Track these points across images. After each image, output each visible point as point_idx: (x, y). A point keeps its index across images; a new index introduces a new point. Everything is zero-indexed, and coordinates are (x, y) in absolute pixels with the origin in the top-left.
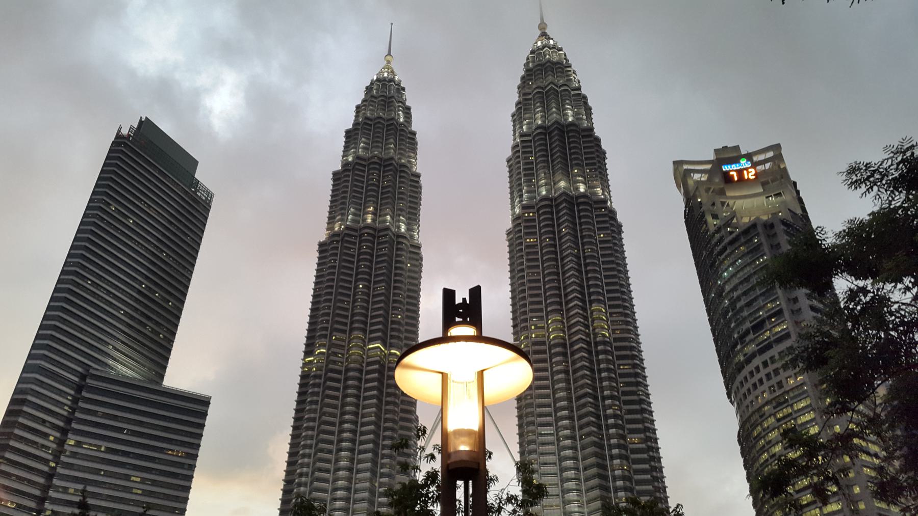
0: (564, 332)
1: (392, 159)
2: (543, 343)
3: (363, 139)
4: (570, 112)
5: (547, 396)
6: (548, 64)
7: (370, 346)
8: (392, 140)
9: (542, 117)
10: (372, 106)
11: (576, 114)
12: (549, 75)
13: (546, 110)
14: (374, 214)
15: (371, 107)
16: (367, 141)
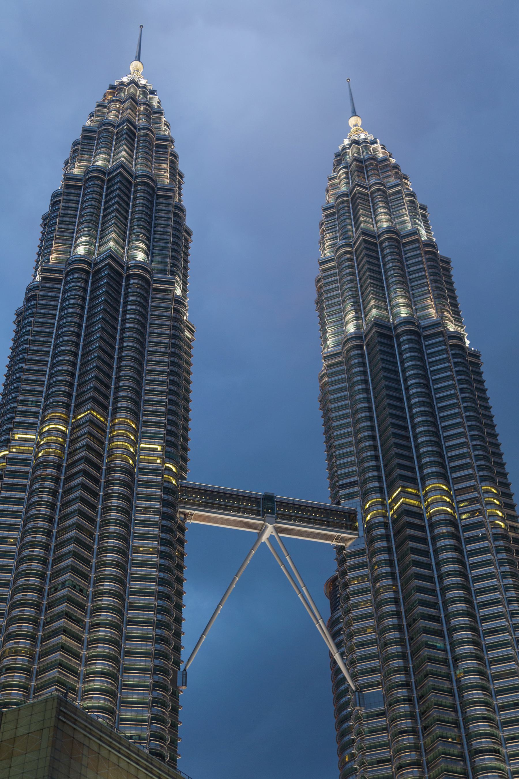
10: (133, 111)
16: (129, 151)
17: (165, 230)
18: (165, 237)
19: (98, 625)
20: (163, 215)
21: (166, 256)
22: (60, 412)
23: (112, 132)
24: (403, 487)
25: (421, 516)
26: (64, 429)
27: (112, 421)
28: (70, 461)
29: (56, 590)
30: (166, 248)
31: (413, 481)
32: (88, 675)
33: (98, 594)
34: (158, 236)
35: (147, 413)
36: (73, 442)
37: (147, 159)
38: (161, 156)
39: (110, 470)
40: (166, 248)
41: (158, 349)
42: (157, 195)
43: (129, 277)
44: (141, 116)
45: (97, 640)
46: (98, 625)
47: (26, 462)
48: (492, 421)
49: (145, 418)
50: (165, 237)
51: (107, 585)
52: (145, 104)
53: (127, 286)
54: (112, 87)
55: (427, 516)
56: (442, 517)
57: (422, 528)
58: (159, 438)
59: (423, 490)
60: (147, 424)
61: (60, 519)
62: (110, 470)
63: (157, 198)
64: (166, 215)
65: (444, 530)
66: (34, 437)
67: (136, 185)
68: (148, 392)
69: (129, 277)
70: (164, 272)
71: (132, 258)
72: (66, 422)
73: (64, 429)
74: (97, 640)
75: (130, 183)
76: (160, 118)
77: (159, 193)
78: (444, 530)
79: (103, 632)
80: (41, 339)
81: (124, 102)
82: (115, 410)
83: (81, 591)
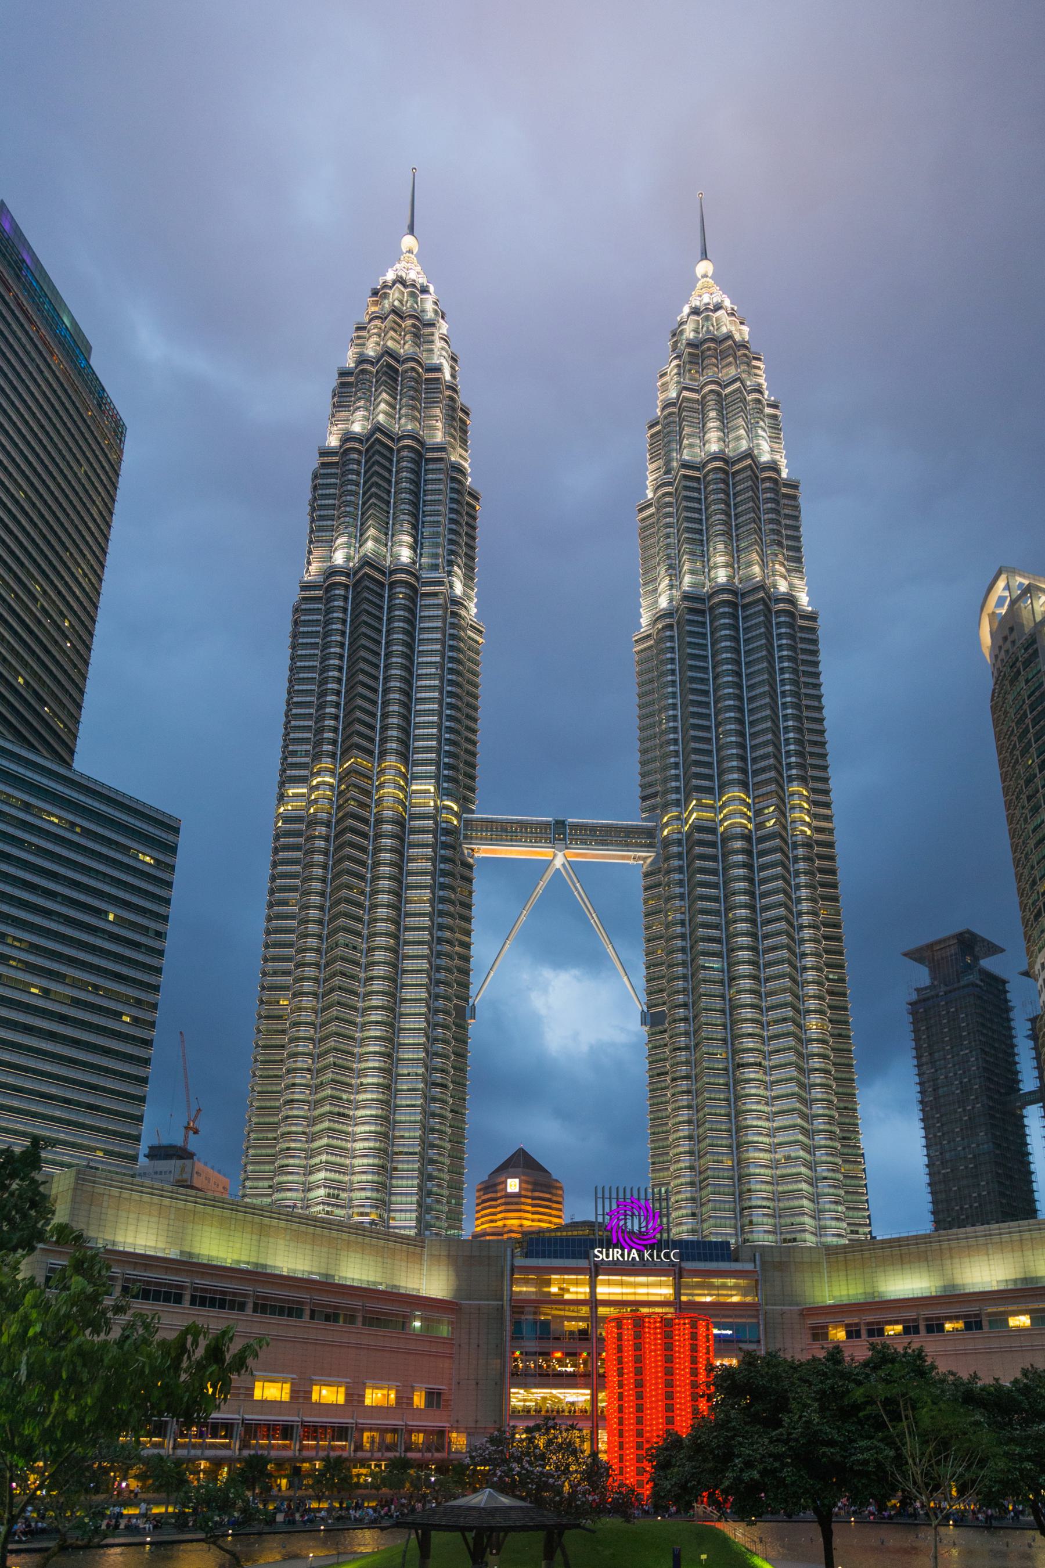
0: (749, 819)
1: (441, 449)
2: (713, 831)
3: (384, 395)
4: (765, 446)
5: (717, 913)
6: (731, 342)
7: (414, 788)
8: (437, 412)
9: (720, 439)
10: (395, 331)
11: (773, 451)
12: (730, 364)
13: (725, 428)
14: (413, 548)
15: (392, 333)
16: (391, 400)
17: (436, 508)
18: (436, 518)
19: (372, 978)
20: (434, 487)
21: (437, 545)
22: (326, 763)
23: (371, 373)
24: (697, 800)
25: (713, 831)
26: (331, 780)
27: (379, 765)
28: (340, 815)
29: (332, 949)
30: (437, 535)
31: (709, 791)
32: (364, 1024)
33: (371, 949)
34: (428, 518)
35: (417, 750)
36: (341, 793)
37: (414, 408)
38: (432, 395)
39: (379, 821)
40: (437, 535)
41: (429, 671)
42: (426, 459)
43: (392, 585)
44: (408, 337)
45: (372, 993)
46: (372, 978)
47: (298, 820)
48: (820, 702)
49: (416, 756)
50: (436, 518)
51: (380, 941)
52: (411, 316)
53: (391, 598)
54: (375, 293)
55: (721, 829)
56: (739, 830)
57: (713, 844)
58: (430, 778)
59: (720, 800)
60: (417, 763)
61: (333, 877)
62: (379, 821)
63: (426, 464)
64: (437, 487)
65: (738, 845)
66: (305, 791)
67: (399, 451)
68: (419, 725)
69: (392, 585)
70: (435, 567)
71: (396, 557)
72: (332, 773)
73: (331, 780)
74: (372, 993)
75: (391, 450)
76: (432, 334)
77: (430, 455)
78: (738, 845)
79: (377, 986)
80: (306, 675)
81: (386, 318)
82: (383, 754)
83: (355, 948)
